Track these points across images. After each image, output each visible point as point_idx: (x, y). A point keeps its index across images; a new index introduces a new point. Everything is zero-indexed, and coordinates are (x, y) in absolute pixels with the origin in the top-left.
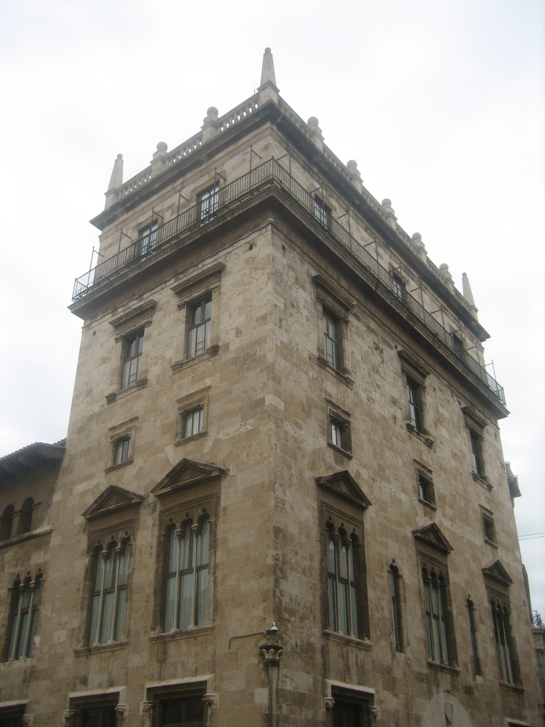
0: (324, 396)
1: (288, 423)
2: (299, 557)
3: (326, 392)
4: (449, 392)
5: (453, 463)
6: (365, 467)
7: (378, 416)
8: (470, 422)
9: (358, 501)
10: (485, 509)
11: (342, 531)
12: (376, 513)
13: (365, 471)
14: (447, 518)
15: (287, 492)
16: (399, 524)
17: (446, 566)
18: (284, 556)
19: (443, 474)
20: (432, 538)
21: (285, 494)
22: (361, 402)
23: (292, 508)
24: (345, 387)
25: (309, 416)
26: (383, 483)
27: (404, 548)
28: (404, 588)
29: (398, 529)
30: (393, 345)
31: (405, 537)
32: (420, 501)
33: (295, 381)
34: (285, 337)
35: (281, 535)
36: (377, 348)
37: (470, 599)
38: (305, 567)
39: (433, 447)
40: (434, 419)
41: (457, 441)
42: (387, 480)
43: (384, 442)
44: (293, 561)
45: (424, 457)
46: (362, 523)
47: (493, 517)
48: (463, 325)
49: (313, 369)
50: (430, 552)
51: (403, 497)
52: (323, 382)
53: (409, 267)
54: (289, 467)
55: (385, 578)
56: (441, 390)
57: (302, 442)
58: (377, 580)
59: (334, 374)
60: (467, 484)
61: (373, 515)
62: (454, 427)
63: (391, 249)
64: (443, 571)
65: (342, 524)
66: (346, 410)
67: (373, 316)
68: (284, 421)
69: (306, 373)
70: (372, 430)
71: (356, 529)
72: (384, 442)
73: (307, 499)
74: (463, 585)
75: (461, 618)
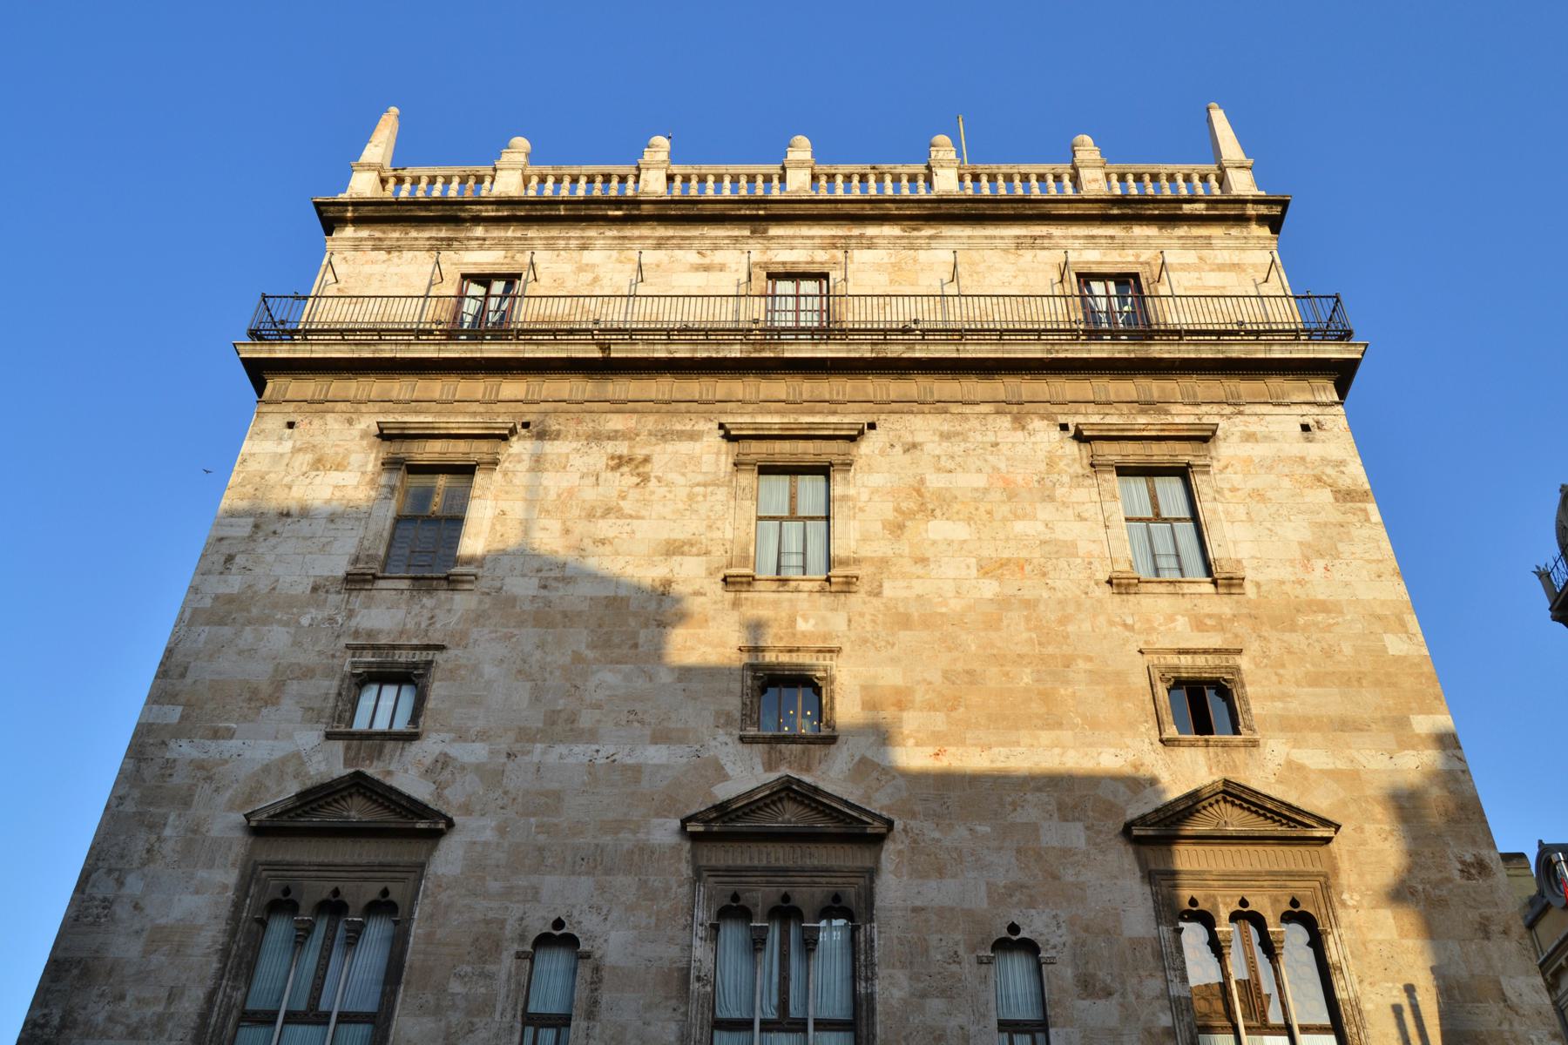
0: (344, 641)
1: (184, 743)
2: (125, 1004)
3: (356, 634)
4: (1005, 422)
5: (989, 588)
6: (482, 736)
7: (584, 606)
8: (1113, 453)
9: (420, 825)
10: (1205, 652)
11: (334, 907)
12: (502, 830)
13: (477, 745)
14: (911, 742)
15: (130, 879)
16: (618, 826)
17: (872, 873)
18: (62, 1018)
19: (905, 636)
20: (790, 816)
21: (121, 883)
22: (512, 600)
23: (136, 907)
24: (442, 595)
25: (272, 700)
26: (561, 749)
27: (620, 880)
28: (596, 983)
29: (607, 839)
30: (702, 426)
31: (645, 851)
32: (742, 739)
33: (240, 653)
34: (234, 583)
35: (75, 972)
36: (619, 462)
37: (1023, 934)
38: (141, 1021)
39: (863, 588)
40: (890, 515)
41: (1020, 527)
42: (592, 736)
43: (590, 654)
44: (100, 1018)
45: (802, 626)
46: (422, 866)
47: (1243, 662)
48: (1152, 231)
49: (320, 605)
50: (779, 855)
51: (655, 754)
52: (351, 614)
53: (856, 231)
54: (155, 826)
55: (503, 976)
56: (946, 436)
57: (226, 762)
58: (455, 987)
59: (404, 584)
60: (1064, 620)
61: (489, 835)
62: (1011, 495)
63: (774, 231)
64: (852, 891)
65: (336, 892)
66: (435, 639)
67: (619, 405)
68: (172, 744)
69: (287, 624)
70: (541, 646)
71: (391, 886)
72: (590, 654)
73: (202, 874)
74: (979, 901)
75: (936, 1004)
